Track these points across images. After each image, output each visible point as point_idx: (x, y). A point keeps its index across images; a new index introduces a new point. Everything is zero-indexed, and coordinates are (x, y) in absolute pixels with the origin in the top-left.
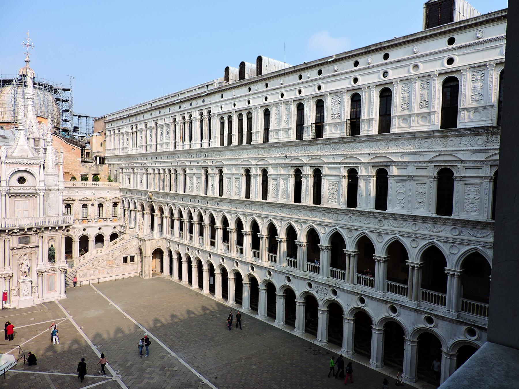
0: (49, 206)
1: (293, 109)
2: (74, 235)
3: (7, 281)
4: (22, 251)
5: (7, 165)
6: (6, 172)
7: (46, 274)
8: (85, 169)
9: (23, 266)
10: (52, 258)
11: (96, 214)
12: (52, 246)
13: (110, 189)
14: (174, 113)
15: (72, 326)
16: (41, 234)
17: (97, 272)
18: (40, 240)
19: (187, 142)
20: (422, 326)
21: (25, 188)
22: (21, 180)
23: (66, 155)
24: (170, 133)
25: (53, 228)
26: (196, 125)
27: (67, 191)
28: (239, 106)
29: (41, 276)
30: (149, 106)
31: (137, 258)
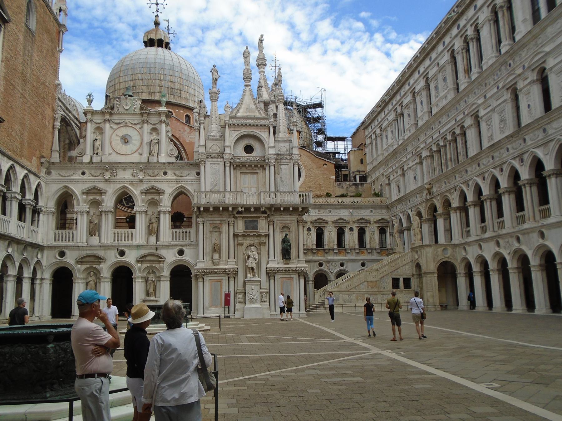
0: (282, 181)
2: (328, 271)
4: (248, 241)
5: (232, 129)
6: (231, 136)
7: (279, 276)
8: (341, 189)
10: (286, 253)
11: (357, 242)
12: (286, 236)
13: (374, 207)
14: (450, 42)
16: (271, 219)
17: (353, 297)
18: (271, 227)
19: (475, 70)
21: (252, 159)
22: (249, 149)
23: (317, 172)
25: (287, 209)
26: (486, 34)
27: (317, 210)
29: (272, 278)
31: (414, 283)
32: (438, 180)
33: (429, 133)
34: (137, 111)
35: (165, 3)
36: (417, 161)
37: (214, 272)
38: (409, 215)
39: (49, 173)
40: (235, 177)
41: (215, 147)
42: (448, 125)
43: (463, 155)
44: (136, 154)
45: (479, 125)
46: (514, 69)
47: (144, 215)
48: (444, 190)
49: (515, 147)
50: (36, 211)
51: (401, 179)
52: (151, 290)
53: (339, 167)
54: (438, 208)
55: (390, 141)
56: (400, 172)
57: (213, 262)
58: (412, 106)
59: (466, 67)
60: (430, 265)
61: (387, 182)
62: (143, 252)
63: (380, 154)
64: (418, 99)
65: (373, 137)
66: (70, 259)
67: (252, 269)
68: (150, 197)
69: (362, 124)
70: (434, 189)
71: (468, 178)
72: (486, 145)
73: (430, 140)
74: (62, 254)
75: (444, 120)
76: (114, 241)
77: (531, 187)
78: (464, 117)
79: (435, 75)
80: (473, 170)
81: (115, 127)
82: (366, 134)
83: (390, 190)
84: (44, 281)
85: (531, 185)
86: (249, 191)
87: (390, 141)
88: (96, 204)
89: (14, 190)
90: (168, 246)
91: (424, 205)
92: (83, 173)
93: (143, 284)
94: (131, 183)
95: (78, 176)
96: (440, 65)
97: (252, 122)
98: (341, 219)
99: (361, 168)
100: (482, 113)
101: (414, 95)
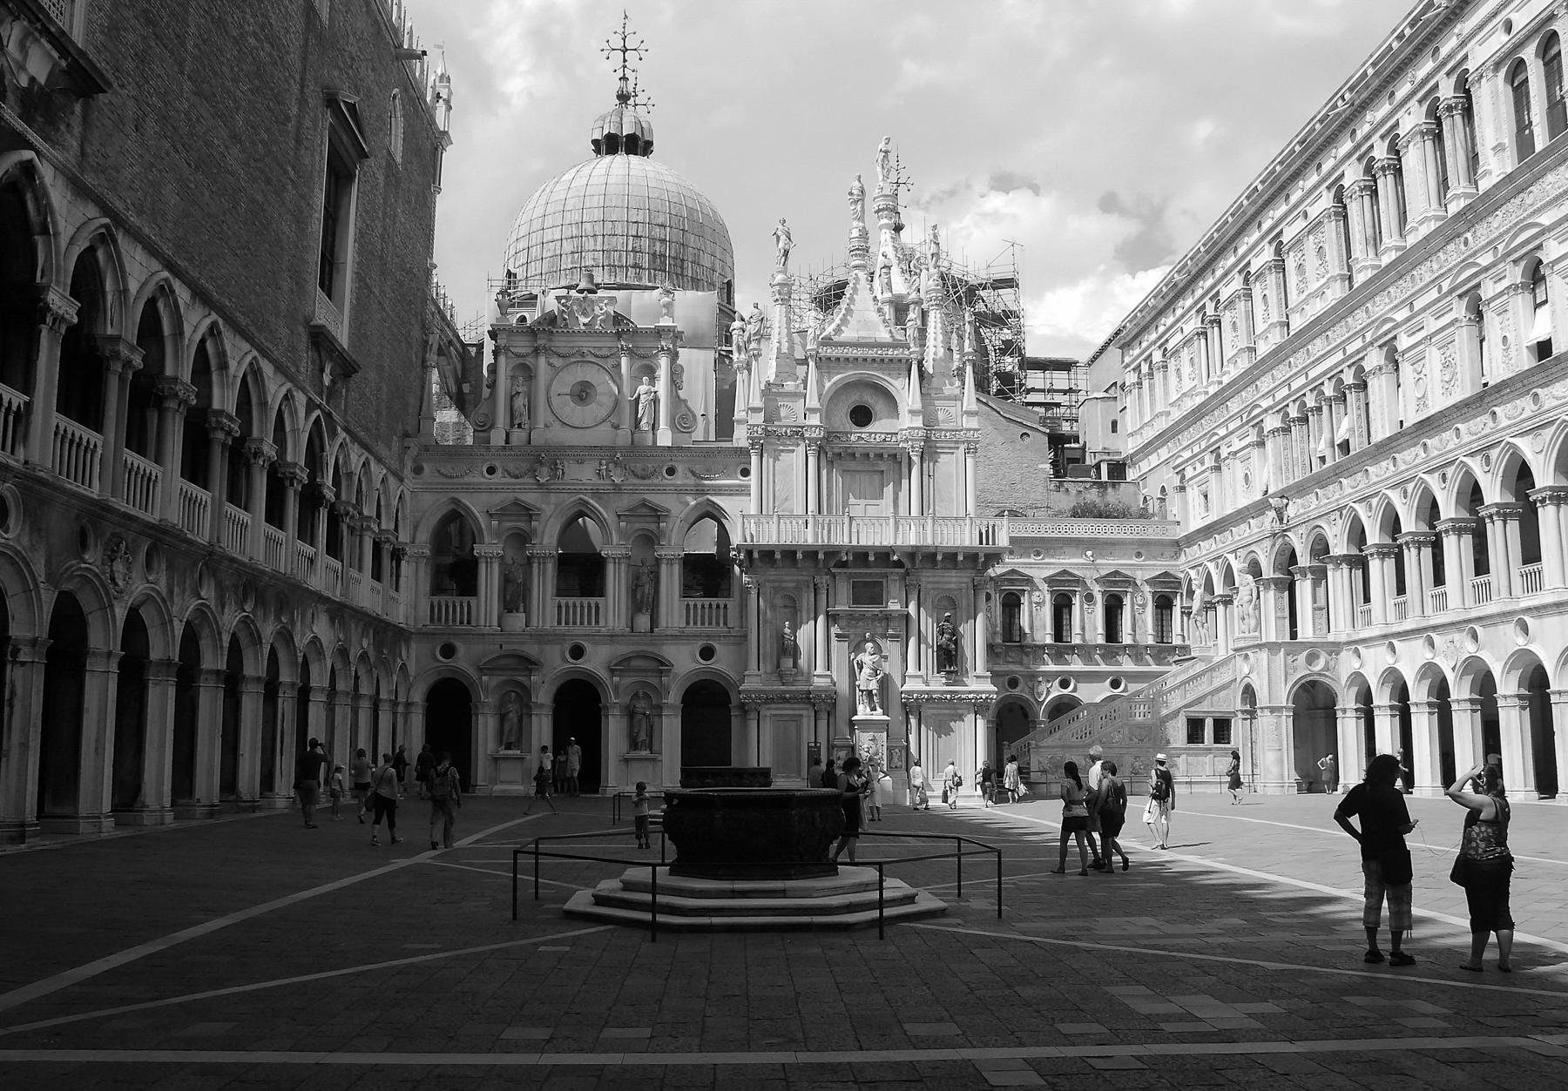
3: (824, 716)
7: (930, 712)
9: (866, 670)
14: (1334, 169)
19: (1390, 240)
24: (1326, 247)
25: (951, 558)
26: (1416, 159)
31: (1238, 729)
32: (1300, 489)
33: (1281, 373)
35: (643, 46)
36: (1253, 438)
37: (782, 699)
38: (1229, 567)
39: (418, 470)
42: (1323, 358)
43: (1361, 435)
44: (606, 427)
45: (1397, 370)
46: (1475, 253)
47: (623, 567)
48: (1314, 514)
49: (1473, 429)
50: (397, 555)
51: (1213, 477)
52: (643, 736)
53: (1057, 441)
54: (1298, 555)
55: (1186, 382)
56: (1209, 461)
57: (781, 676)
58: (1241, 305)
59: (1370, 231)
61: (1177, 482)
62: (623, 649)
63: (1161, 414)
64: (1257, 290)
65: (1145, 368)
66: (464, 661)
67: (870, 693)
68: (637, 526)
69: (1117, 334)
70: (1291, 511)
71: (1368, 492)
73: (1284, 392)
74: (449, 651)
75: (1318, 347)
76: (559, 623)
77: (1505, 522)
78: (1364, 348)
79: (1298, 242)
80: (1380, 471)
81: (557, 362)
82: (1127, 360)
83: (1185, 503)
84: (413, 709)
85: (1505, 518)
87: (1187, 385)
88: (521, 539)
89: (366, 512)
91: (1267, 543)
92: (491, 471)
93: (624, 722)
94: (596, 494)
95: (479, 477)
96: (1312, 216)
97: (871, 353)
98: (1064, 572)
100: (1403, 342)
101: (1246, 281)
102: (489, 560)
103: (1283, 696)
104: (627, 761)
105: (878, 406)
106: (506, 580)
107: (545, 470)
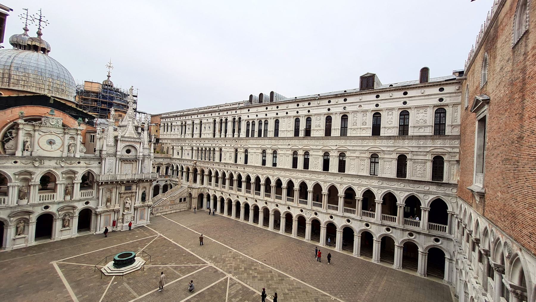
1: (293, 121)
4: (126, 195)
10: (143, 199)
15: (165, 239)
20: (364, 228)
22: (128, 151)
25: (147, 181)
26: (230, 125)
28: (260, 116)
30: (197, 111)
31: (188, 199)
33: (198, 142)
34: (61, 126)
36: (190, 148)
37: (107, 211)
40: (121, 165)
41: (112, 151)
44: (59, 151)
60: (195, 194)
61: (172, 147)
62: (61, 205)
72: (223, 161)
75: (207, 142)
86: (127, 172)
90: (80, 201)
94: (55, 168)
99: (156, 134)
100: (223, 150)
102: (13, 187)
103: (197, 196)
104: (61, 231)
105: (133, 150)
106: (20, 191)
107: (37, 163)
